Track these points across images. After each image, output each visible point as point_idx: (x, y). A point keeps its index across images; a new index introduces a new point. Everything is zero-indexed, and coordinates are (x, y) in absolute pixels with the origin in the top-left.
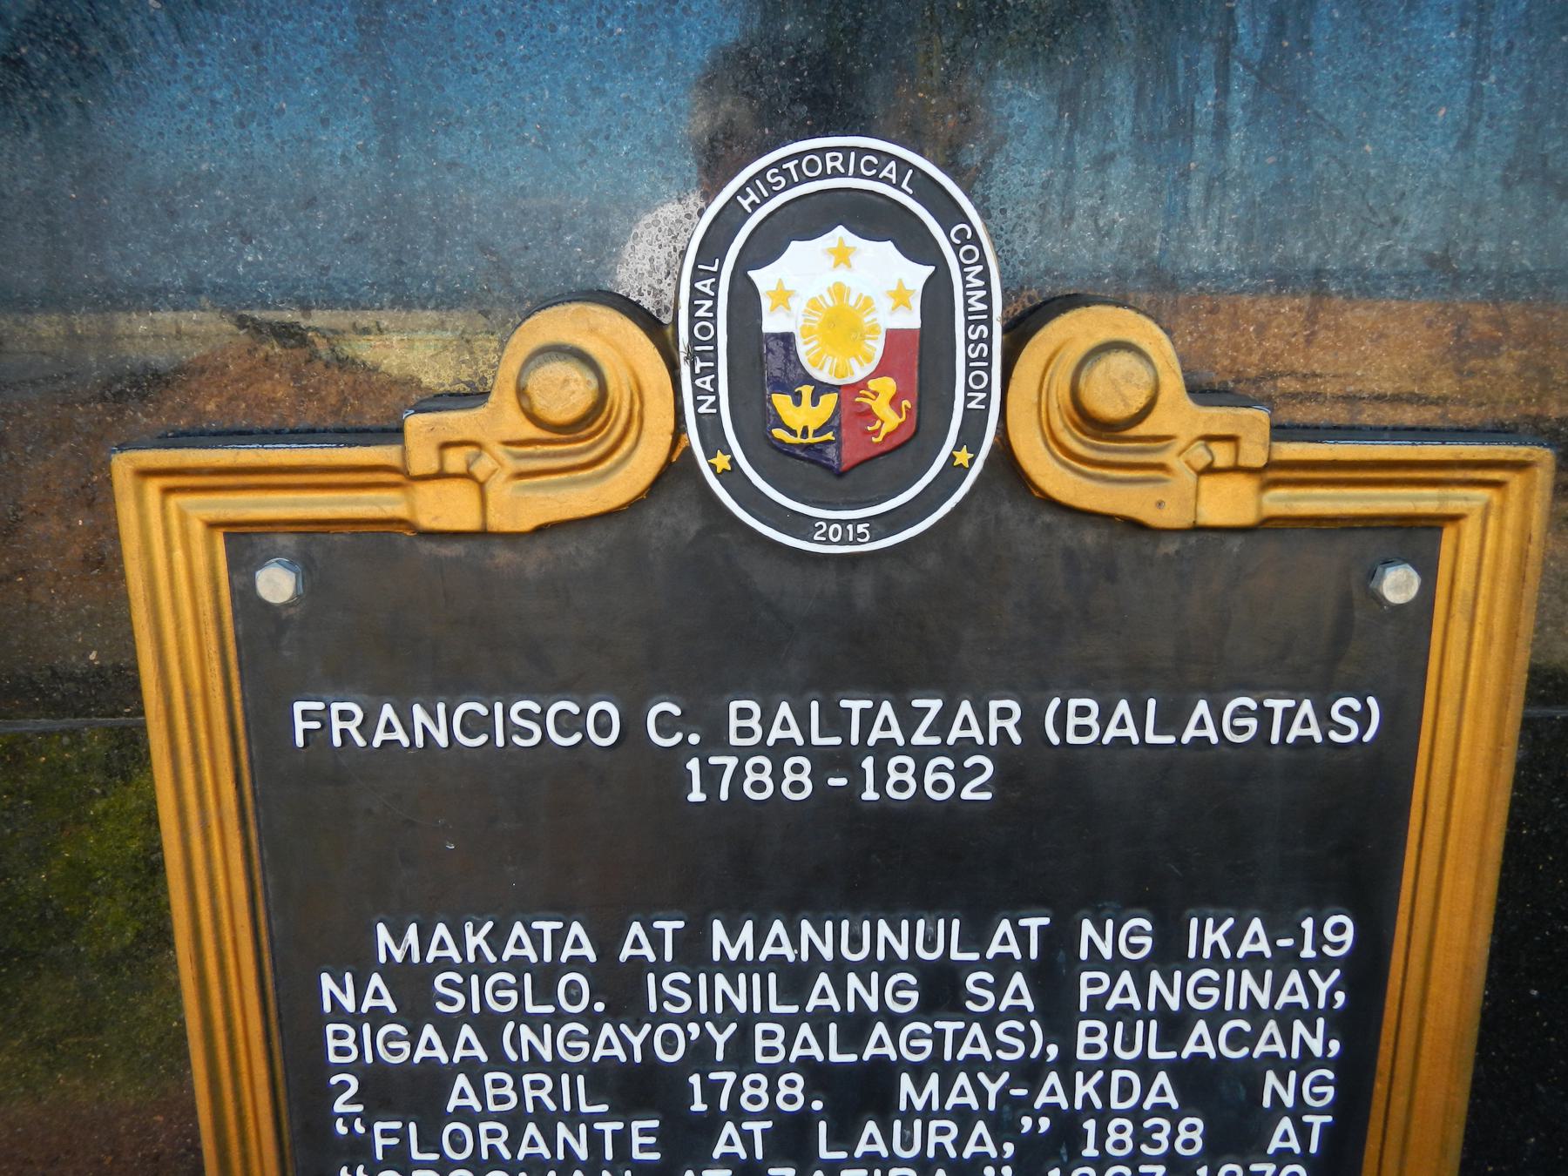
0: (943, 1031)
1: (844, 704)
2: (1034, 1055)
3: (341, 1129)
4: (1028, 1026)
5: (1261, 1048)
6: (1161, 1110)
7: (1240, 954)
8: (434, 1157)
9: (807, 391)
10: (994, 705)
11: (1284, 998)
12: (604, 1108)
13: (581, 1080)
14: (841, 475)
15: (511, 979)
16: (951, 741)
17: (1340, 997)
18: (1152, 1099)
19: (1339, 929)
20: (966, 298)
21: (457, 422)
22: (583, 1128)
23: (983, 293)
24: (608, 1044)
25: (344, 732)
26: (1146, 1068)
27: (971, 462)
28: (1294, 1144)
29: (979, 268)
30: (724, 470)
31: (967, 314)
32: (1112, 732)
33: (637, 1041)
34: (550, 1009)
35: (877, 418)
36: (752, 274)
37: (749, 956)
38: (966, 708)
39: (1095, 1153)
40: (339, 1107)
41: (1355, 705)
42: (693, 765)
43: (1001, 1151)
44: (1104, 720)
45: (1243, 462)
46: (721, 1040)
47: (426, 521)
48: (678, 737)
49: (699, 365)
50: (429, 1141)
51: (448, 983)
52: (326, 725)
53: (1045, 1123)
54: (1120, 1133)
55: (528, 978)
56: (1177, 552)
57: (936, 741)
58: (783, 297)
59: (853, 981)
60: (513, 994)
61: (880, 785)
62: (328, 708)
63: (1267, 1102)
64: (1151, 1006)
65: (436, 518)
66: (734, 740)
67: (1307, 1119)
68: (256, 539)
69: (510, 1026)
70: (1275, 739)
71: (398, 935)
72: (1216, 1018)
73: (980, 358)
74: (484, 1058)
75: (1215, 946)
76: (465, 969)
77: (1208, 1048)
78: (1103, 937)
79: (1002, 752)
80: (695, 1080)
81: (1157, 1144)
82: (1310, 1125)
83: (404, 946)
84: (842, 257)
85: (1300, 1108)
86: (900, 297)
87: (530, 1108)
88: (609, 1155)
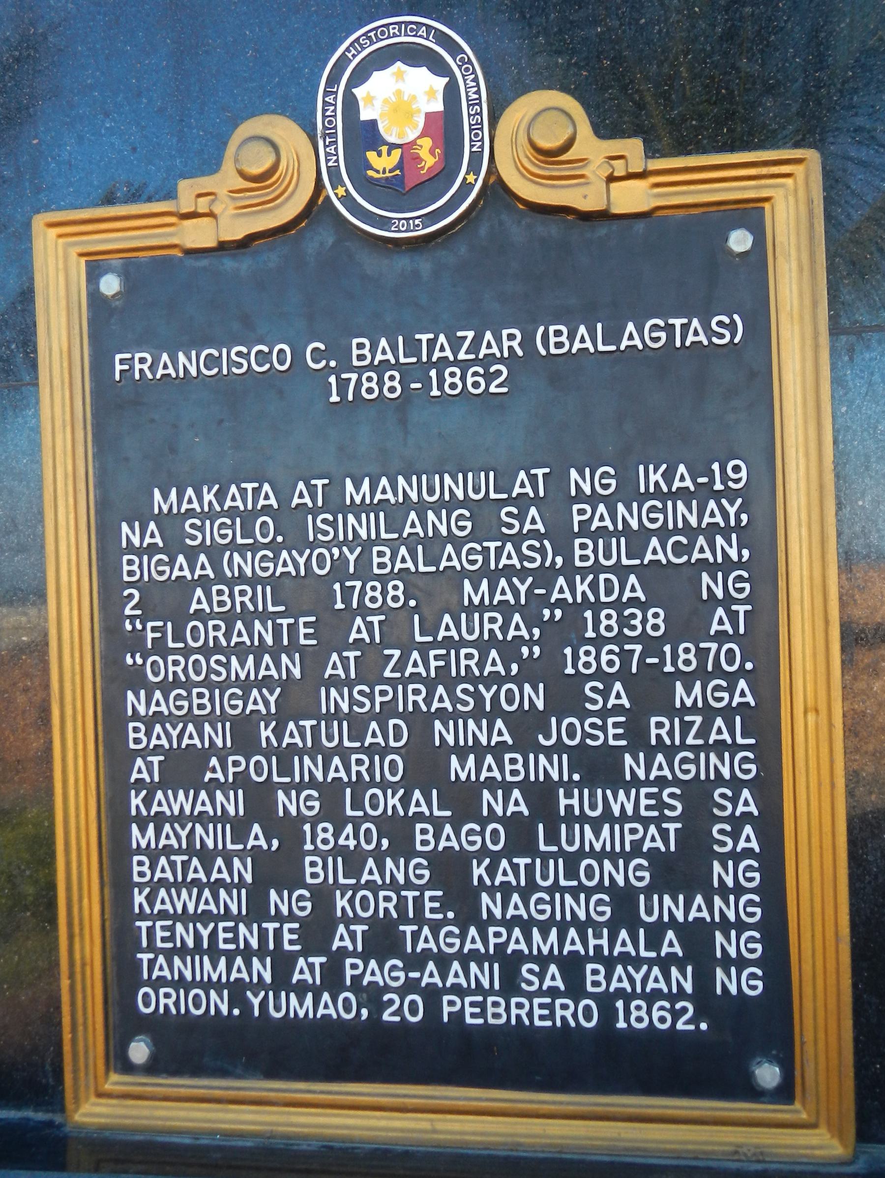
0: (488, 548)
1: (417, 336)
2: (547, 564)
3: (129, 627)
4: (542, 545)
5: (696, 555)
6: (634, 602)
7: (674, 489)
8: (181, 645)
9: (384, 149)
10: (505, 333)
11: (707, 520)
12: (282, 608)
13: (268, 588)
14: (404, 194)
15: (229, 522)
16: (481, 356)
17: (744, 517)
18: (627, 594)
19: (737, 469)
20: (467, 93)
21: (206, 183)
22: (270, 623)
23: (476, 89)
24: (285, 564)
25: (141, 371)
26: (621, 572)
27: (476, 180)
28: (728, 627)
29: (473, 76)
30: (342, 196)
31: (468, 101)
32: (577, 345)
33: (302, 561)
34: (251, 541)
35: (422, 160)
36: (354, 90)
37: (368, 501)
38: (488, 336)
39: (594, 635)
40: (128, 611)
41: (727, 320)
42: (332, 379)
43: (531, 635)
44: (571, 337)
45: (630, 170)
46: (352, 558)
47: (190, 244)
48: (324, 363)
49: (328, 140)
50: (178, 636)
51: (192, 526)
52: (132, 368)
53: (558, 613)
54: (609, 620)
55: (238, 520)
56: (606, 235)
57: (472, 356)
58: (370, 99)
59: (431, 515)
60: (230, 532)
61: (440, 387)
62: (133, 358)
63: (705, 596)
64: (620, 527)
65: (193, 241)
66: (356, 363)
67: (734, 607)
68: (101, 263)
69: (228, 553)
70: (678, 344)
71: (165, 496)
72: (663, 534)
73: (477, 124)
74: (212, 576)
75: (657, 483)
76: (203, 516)
77: (660, 556)
78: (584, 480)
79: (511, 359)
80: (337, 586)
81: (633, 628)
82: (737, 612)
83: (169, 502)
84: (400, 76)
85: (728, 601)
86: (431, 93)
87: (238, 610)
88: (286, 642)
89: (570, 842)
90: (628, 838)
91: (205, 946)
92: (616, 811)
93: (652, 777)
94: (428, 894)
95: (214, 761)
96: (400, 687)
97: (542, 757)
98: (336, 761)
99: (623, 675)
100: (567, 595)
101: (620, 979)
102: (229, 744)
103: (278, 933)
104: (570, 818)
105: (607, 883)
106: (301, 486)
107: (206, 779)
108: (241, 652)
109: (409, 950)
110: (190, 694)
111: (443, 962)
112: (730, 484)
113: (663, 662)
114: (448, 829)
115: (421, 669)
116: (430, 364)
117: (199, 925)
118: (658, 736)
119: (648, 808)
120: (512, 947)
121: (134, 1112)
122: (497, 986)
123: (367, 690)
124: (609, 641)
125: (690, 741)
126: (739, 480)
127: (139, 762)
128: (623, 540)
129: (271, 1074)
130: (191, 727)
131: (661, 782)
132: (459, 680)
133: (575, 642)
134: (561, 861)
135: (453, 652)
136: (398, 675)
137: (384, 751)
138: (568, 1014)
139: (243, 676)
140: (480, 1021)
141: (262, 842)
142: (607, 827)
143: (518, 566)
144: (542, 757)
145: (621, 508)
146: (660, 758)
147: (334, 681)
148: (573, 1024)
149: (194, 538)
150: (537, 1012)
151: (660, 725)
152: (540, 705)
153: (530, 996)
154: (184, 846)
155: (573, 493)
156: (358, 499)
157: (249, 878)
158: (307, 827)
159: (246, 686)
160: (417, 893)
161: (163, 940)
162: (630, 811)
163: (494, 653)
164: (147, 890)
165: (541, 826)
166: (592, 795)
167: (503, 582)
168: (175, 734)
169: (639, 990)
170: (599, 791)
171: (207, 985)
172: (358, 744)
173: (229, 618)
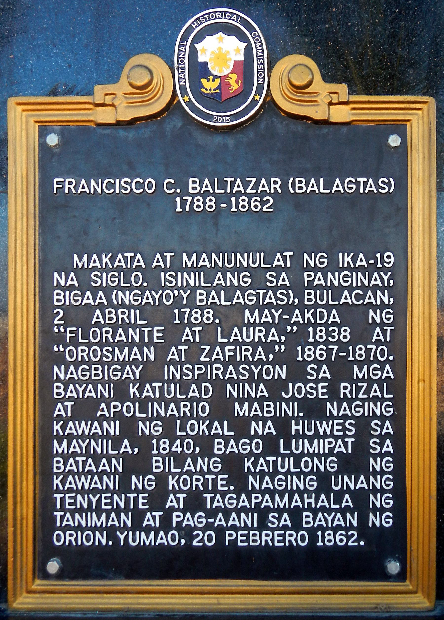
2: (290, 303)
3: (56, 330)
4: (288, 292)
5: (367, 301)
6: (334, 323)
10: (272, 180)
12: (145, 322)
15: (116, 274)
17: (392, 282)
18: (331, 319)
28: (381, 338)
33: (157, 297)
39: (313, 340)
40: (56, 322)
41: (386, 181)
43: (280, 339)
46: (185, 296)
47: (100, 121)
51: (96, 275)
53: (295, 328)
54: (321, 332)
59: (229, 275)
63: (370, 322)
64: (329, 285)
66: (191, 191)
67: (385, 328)
69: (115, 291)
70: (362, 191)
76: (102, 270)
77: (349, 300)
80: (176, 311)
87: (120, 322)
89: (297, 449)
90: (327, 446)
91: (94, 507)
92: (321, 432)
93: (340, 415)
94: (220, 477)
95: (103, 405)
96: (209, 366)
97: (283, 404)
98: (172, 405)
99: (328, 361)
100: (300, 319)
101: (320, 520)
102: (112, 396)
103: (136, 499)
104: (297, 436)
105: (315, 470)
106: (158, 256)
107: (98, 415)
108: (121, 345)
109: (209, 507)
110: (90, 368)
111: (227, 513)
112: (385, 264)
113: (348, 355)
114: (232, 442)
115: (221, 357)
116: (231, 194)
117: (91, 496)
118: (344, 393)
119: (338, 430)
120: (264, 504)
121: (49, 601)
122: (255, 525)
123: (191, 367)
124: (321, 343)
125: (360, 396)
126: (390, 262)
127: (60, 405)
128: (330, 291)
129: (129, 577)
130: (90, 386)
131: (345, 417)
132: (241, 362)
133: (303, 344)
134: (291, 458)
135: (238, 348)
136: (208, 359)
137: (199, 400)
138: (292, 539)
139: (121, 359)
140: (246, 544)
141: (129, 450)
142: (316, 440)
143: (275, 303)
144: (283, 404)
145: (329, 274)
146: (345, 404)
147: (172, 362)
148: (295, 544)
149: (96, 282)
150: (276, 538)
151: (345, 388)
152: (284, 376)
153: (273, 530)
154: (84, 452)
155: (305, 266)
156: (189, 265)
157: (120, 469)
158: (155, 441)
159: (123, 364)
160: (214, 477)
161: (70, 504)
162: (328, 432)
163: (260, 349)
164: (61, 477)
165: (282, 440)
166: (309, 424)
167: (266, 311)
168: (81, 390)
169: (330, 525)
170: (313, 422)
171: (94, 529)
172: (185, 397)
173: (115, 327)
